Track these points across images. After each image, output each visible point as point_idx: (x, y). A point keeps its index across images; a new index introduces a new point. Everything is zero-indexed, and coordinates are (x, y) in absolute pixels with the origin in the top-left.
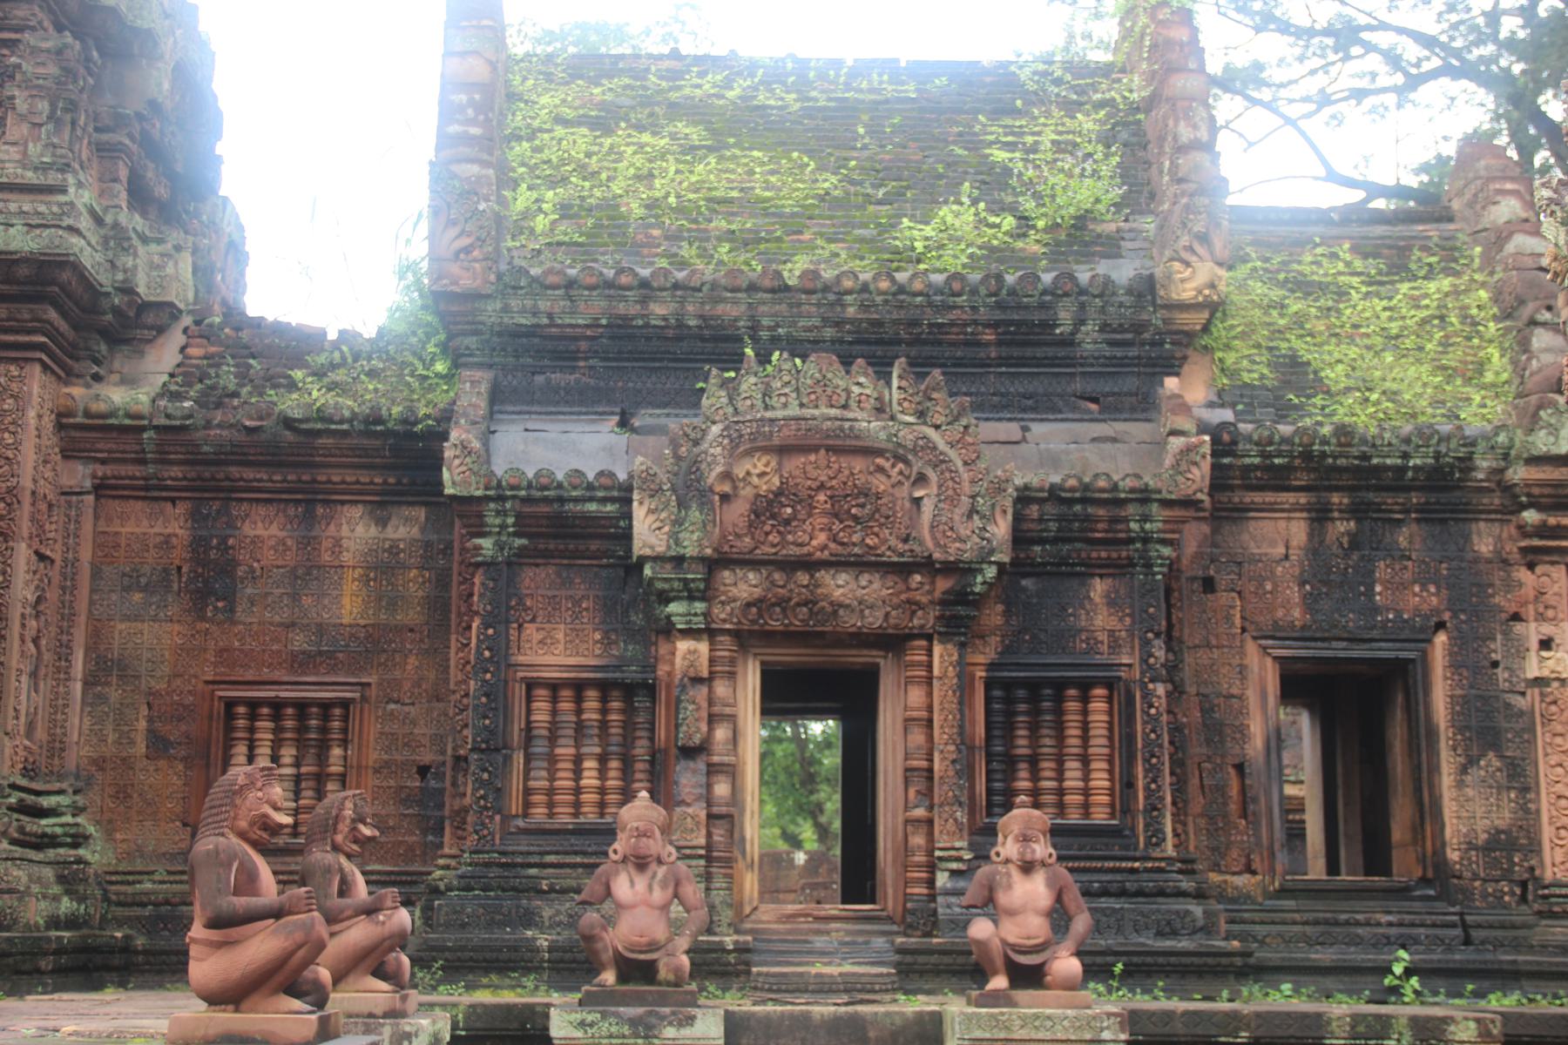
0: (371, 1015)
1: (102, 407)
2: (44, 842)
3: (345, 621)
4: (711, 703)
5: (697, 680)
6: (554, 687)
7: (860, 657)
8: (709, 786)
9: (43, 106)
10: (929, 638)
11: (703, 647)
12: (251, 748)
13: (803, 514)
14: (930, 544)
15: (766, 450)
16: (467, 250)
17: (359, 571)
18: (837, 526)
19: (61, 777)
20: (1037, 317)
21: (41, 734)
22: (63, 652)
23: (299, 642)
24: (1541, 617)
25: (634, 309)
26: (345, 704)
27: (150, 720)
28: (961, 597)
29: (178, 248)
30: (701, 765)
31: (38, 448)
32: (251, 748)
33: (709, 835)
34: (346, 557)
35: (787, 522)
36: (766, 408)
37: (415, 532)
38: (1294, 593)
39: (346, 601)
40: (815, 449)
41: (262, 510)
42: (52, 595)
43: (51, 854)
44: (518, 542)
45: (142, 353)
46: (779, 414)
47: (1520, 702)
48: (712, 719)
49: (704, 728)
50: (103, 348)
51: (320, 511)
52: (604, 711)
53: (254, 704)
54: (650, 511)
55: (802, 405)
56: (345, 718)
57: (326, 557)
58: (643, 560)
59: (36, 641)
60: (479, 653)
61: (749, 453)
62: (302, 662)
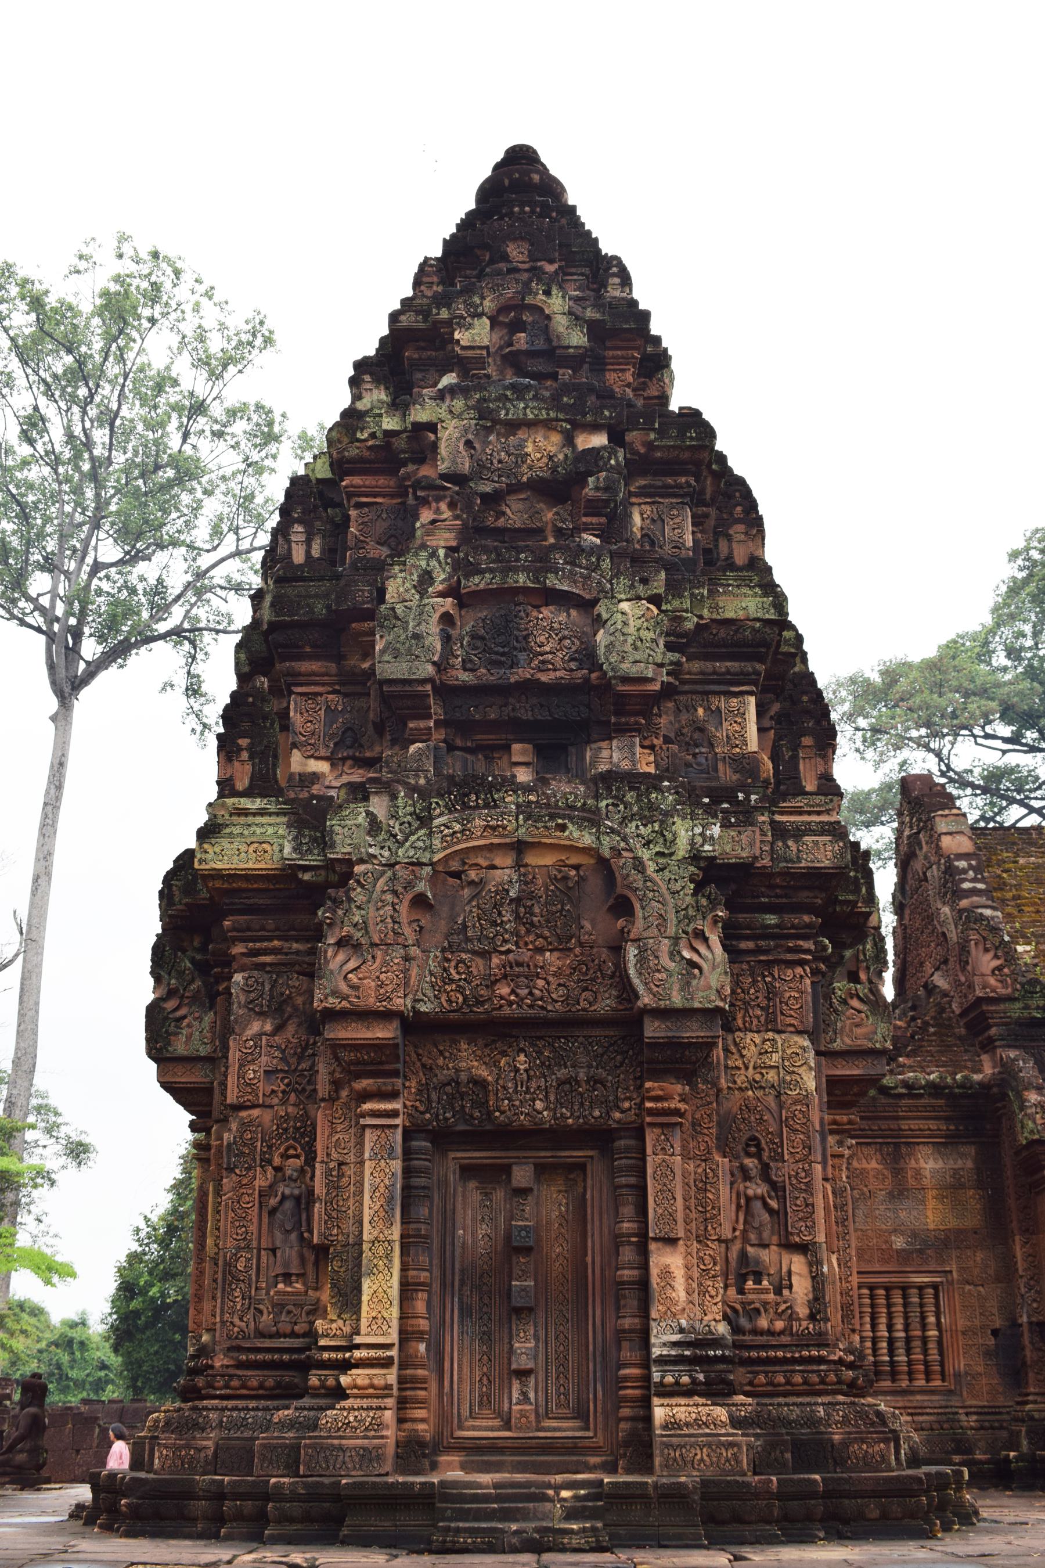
3: (932, 1227)
16: (999, 968)
17: (934, 1192)
23: (899, 1243)
26: (935, 1287)
34: (926, 1182)
37: (970, 1164)
39: (929, 1213)
41: (865, 1150)
51: (904, 1150)
56: (936, 1296)
57: (912, 1182)
62: (904, 1256)
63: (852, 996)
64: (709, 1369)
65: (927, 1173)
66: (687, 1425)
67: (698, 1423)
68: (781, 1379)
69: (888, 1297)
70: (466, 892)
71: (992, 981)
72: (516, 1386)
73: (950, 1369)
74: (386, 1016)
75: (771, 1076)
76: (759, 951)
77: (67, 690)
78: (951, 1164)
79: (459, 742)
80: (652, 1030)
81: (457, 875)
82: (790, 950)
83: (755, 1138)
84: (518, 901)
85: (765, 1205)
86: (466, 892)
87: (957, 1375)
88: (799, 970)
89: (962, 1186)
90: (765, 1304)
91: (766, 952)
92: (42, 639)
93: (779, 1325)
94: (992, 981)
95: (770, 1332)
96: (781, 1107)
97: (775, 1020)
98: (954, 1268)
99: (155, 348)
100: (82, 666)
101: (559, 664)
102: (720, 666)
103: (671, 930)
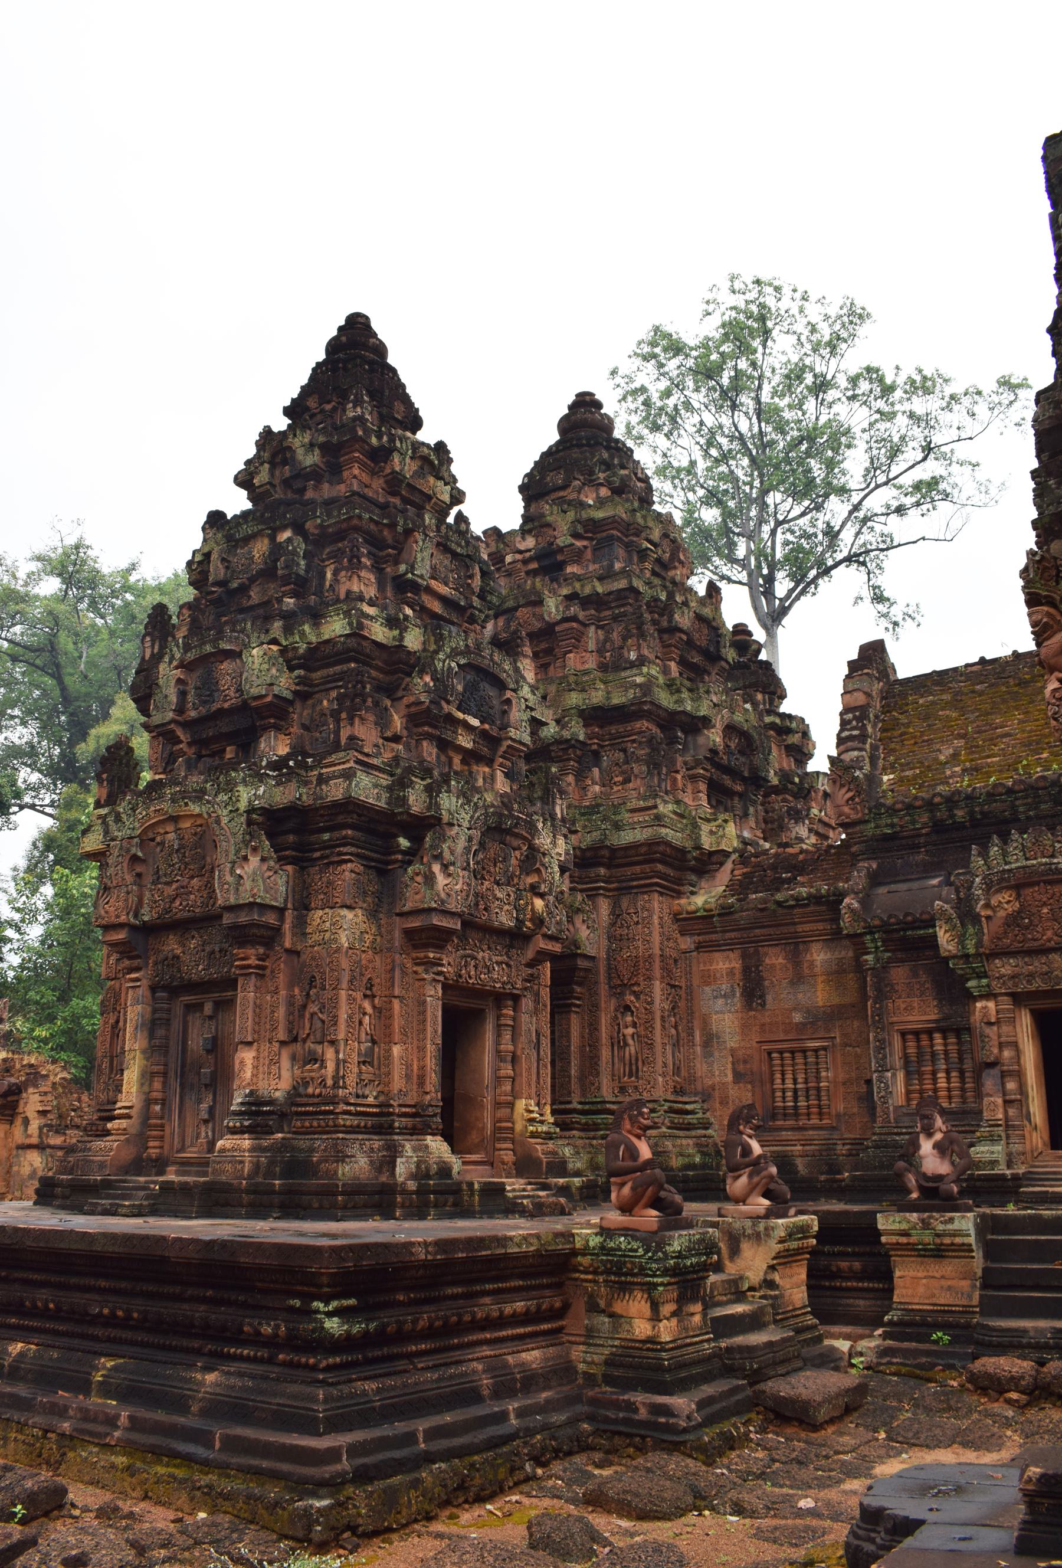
0: (759, 1217)
1: (692, 908)
2: (689, 1127)
3: (821, 1004)
4: (999, 1037)
5: (990, 1024)
6: (917, 1033)
8: (1003, 1084)
9: (644, 768)
11: (991, 1005)
12: (783, 1075)
13: (1036, 922)
15: (1008, 888)
16: (852, 799)
19: (696, 1095)
21: (683, 1073)
22: (691, 1034)
23: (797, 1017)
26: (825, 1049)
27: (733, 1063)
29: (726, 821)
30: (995, 1072)
31: (662, 934)
32: (783, 1075)
33: (1006, 1112)
34: (818, 970)
35: (1027, 928)
36: (1006, 863)
39: (819, 993)
40: (1038, 883)
42: (682, 1004)
43: (693, 1133)
45: (714, 877)
46: (1013, 866)
48: (1001, 1046)
49: (996, 1051)
50: (694, 877)
51: (801, 947)
52: (945, 1045)
53: (781, 1052)
54: (946, 931)
55: (1027, 859)
57: (806, 971)
58: (946, 959)
59: (676, 1027)
62: (801, 1027)
63: (417, 874)
65: (818, 963)
67: (233, 1149)
68: (307, 1124)
69: (793, 1058)
70: (158, 849)
71: (846, 809)
72: (203, 1129)
73: (834, 1112)
74: (121, 926)
76: (322, 858)
77: (769, 622)
78: (837, 955)
79: (204, 752)
80: (227, 919)
81: (153, 840)
84: (178, 851)
86: (158, 849)
87: (838, 1115)
89: (844, 971)
90: (312, 1079)
91: (327, 857)
92: (746, 588)
93: (318, 1091)
94: (846, 809)
95: (313, 1096)
98: (838, 1035)
99: (781, 351)
100: (777, 602)
101: (232, 694)
102: (331, 671)
103: (232, 857)
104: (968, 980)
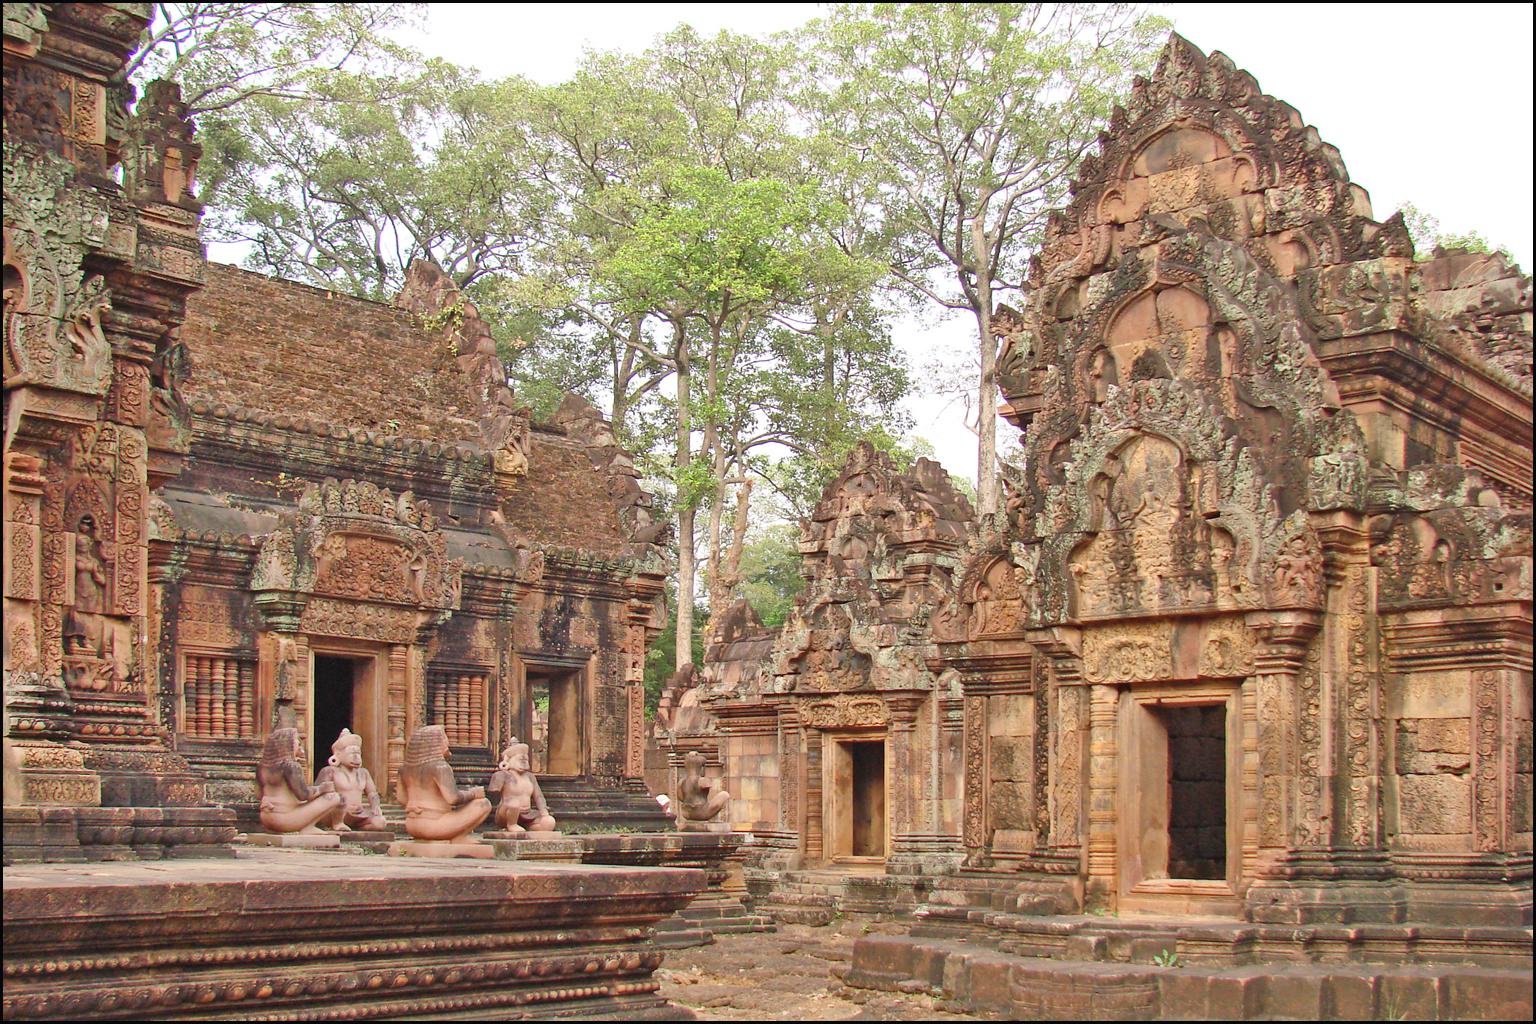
7: (362, 653)
10: (407, 646)
14: (421, 595)
15: (341, 534)
18: (373, 582)
20: (435, 468)
24: (634, 652)
25: (222, 430)
28: (428, 627)
38: (536, 632)
40: (365, 537)
44: (186, 571)
47: (623, 692)
60: (162, 638)
61: (333, 536)
64: (63, 717)
66: (46, 763)
75: (108, 462)
82: (135, 349)
83: (89, 517)
85: (93, 576)
88: (139, 370)
96: (115, 494)
97: (115, 412)
104: (280, 615)
